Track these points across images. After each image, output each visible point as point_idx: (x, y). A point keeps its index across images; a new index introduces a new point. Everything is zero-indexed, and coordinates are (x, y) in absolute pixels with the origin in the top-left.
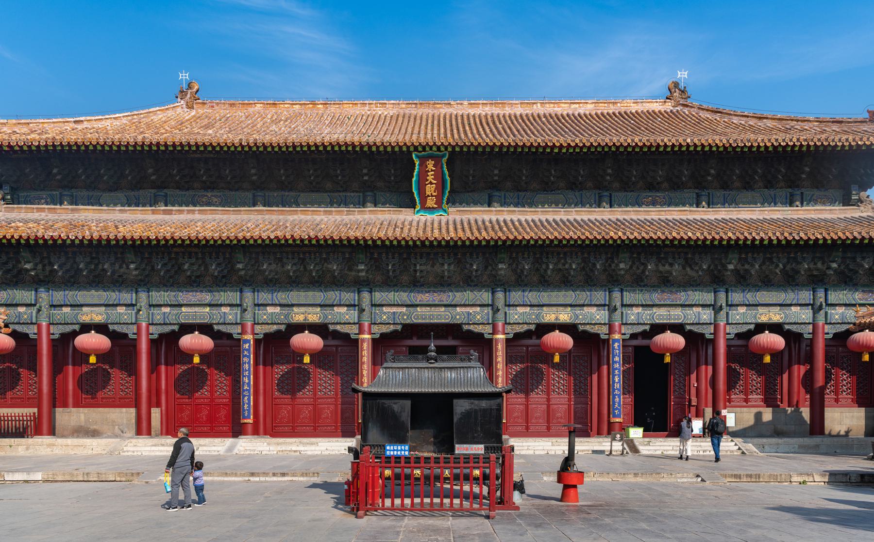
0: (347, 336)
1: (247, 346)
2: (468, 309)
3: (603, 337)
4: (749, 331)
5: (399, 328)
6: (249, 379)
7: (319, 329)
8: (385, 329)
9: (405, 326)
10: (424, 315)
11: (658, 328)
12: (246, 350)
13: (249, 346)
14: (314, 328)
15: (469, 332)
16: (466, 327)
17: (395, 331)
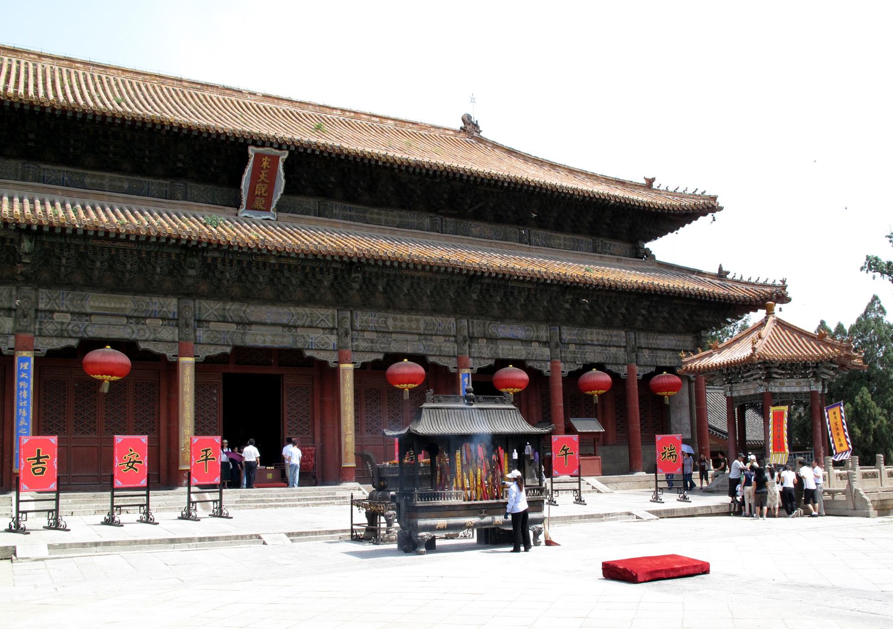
0: (161, 358)
1: (25, 366)
2: (315, 332)
3: (453, 371)
4: (579, 370)
5: (228, 350)
6: (28, 412)
7: (126, 346)
8: (214, 351)
9: (237, 349)
10: (261, 338)
11: (502, 363)
12: (25, 371)
13: (29, 366)
14: (118, 345)
15: (311, 359)
16: (308, 353)
17: (224, 355)
